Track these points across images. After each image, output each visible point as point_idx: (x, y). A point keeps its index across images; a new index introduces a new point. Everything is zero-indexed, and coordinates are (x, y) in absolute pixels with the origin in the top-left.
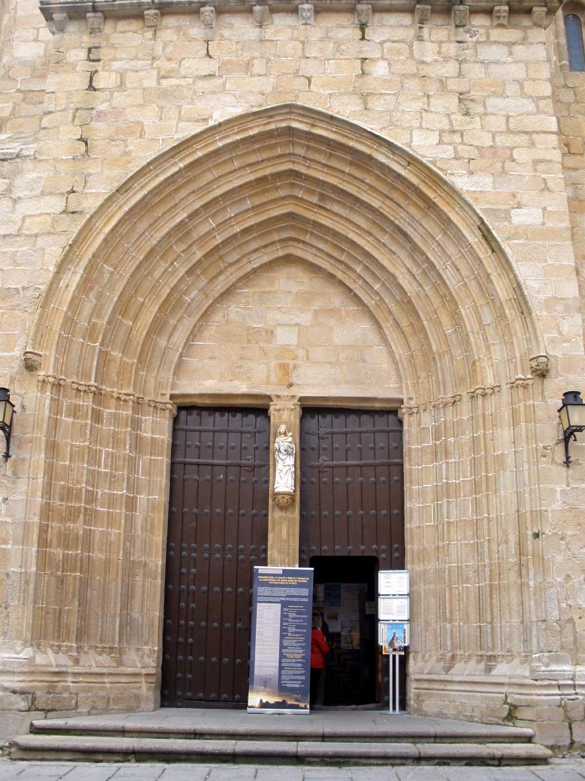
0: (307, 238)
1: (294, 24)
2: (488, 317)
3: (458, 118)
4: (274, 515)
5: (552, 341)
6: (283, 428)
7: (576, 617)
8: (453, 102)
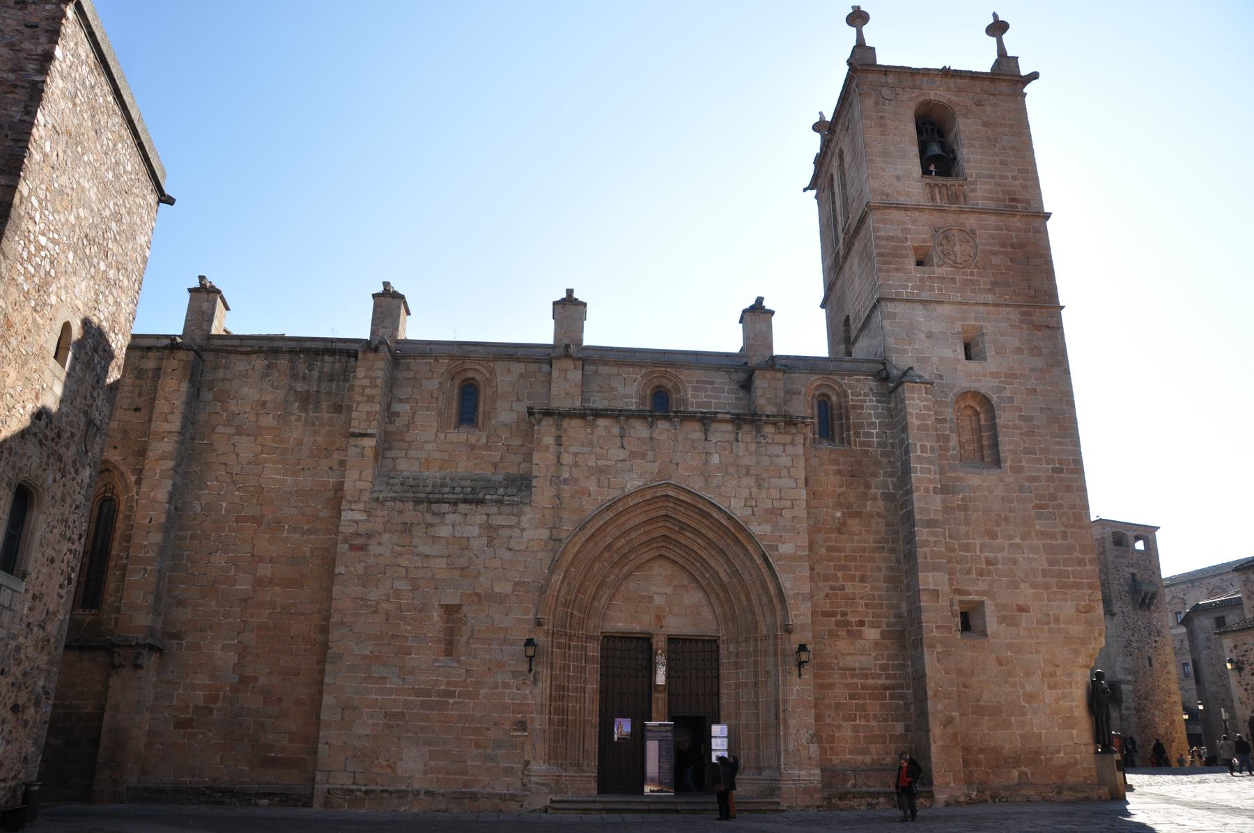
0: (671, 547)
1: (669, 428)
2: (765, 601)
3: (754, 490)
4: (655, 695)
5: (796, 616)
6: (660, 652)
7: (801, 749)
8: (752, 481)
